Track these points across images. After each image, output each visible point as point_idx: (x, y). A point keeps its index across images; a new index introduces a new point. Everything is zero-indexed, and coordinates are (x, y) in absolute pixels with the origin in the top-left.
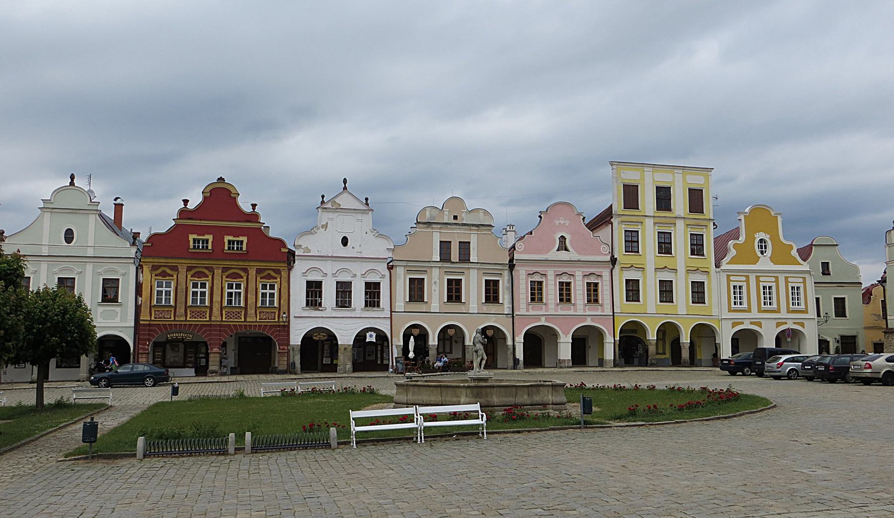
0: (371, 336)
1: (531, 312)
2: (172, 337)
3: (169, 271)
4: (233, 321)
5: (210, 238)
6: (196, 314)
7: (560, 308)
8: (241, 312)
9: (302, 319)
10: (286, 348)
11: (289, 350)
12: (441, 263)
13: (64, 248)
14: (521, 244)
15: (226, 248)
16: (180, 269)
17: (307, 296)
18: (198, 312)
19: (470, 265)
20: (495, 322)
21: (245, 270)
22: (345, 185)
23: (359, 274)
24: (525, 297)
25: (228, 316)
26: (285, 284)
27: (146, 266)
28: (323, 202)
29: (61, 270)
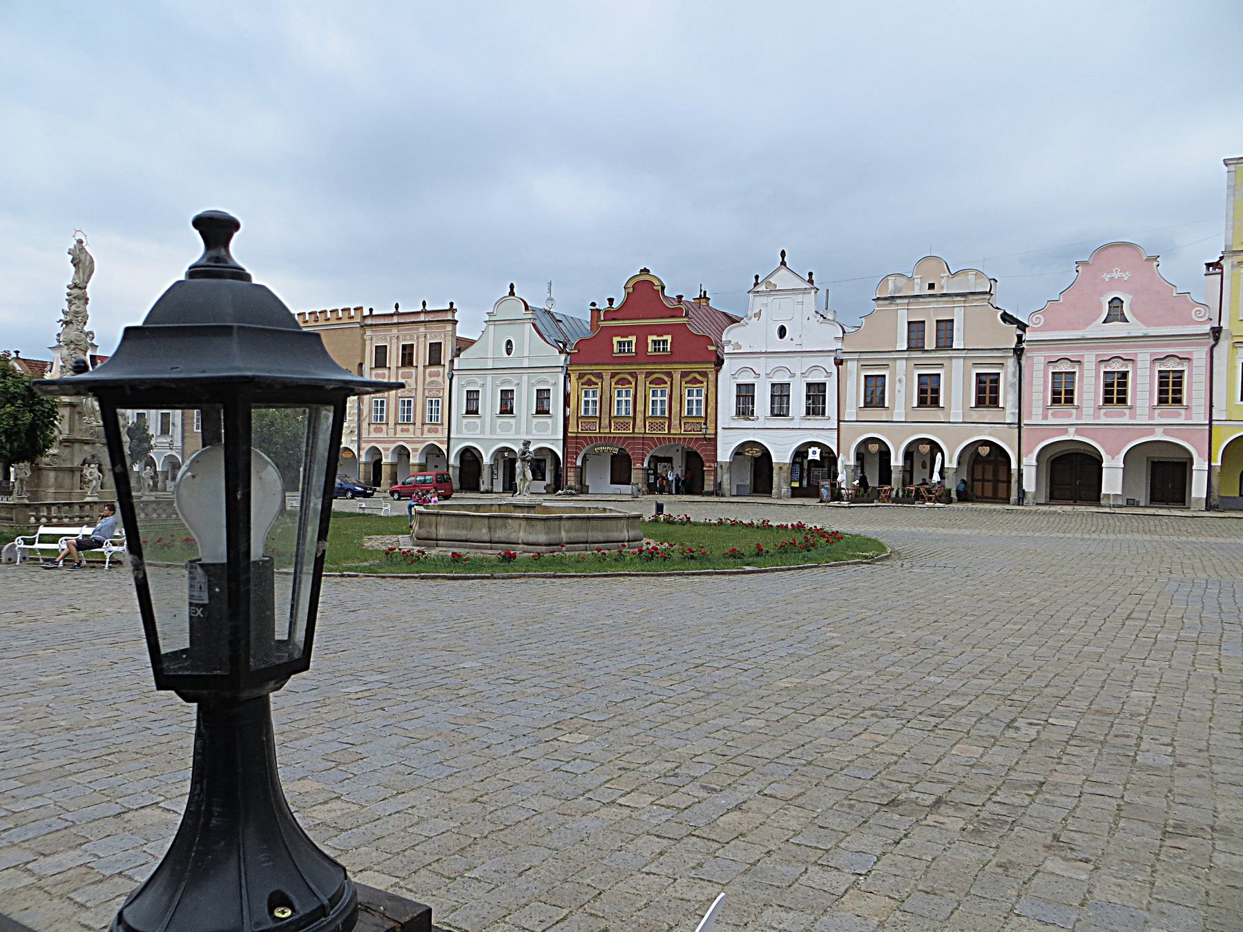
0: (814, 453)
1: (1051, 420)
7: (1053, 414)
10: (712, 465)
11: (716, 468)
12: (908, 353)
14: (1038, 316)
17: (738, 403)
19: (951, 353)
20: (990, 434)
21: (670, 375)
22: (783, 258)
23: (798, 374)
24: (1041, 398)
26: (712, 389)
28: (756, 284)
29: (503, 383)
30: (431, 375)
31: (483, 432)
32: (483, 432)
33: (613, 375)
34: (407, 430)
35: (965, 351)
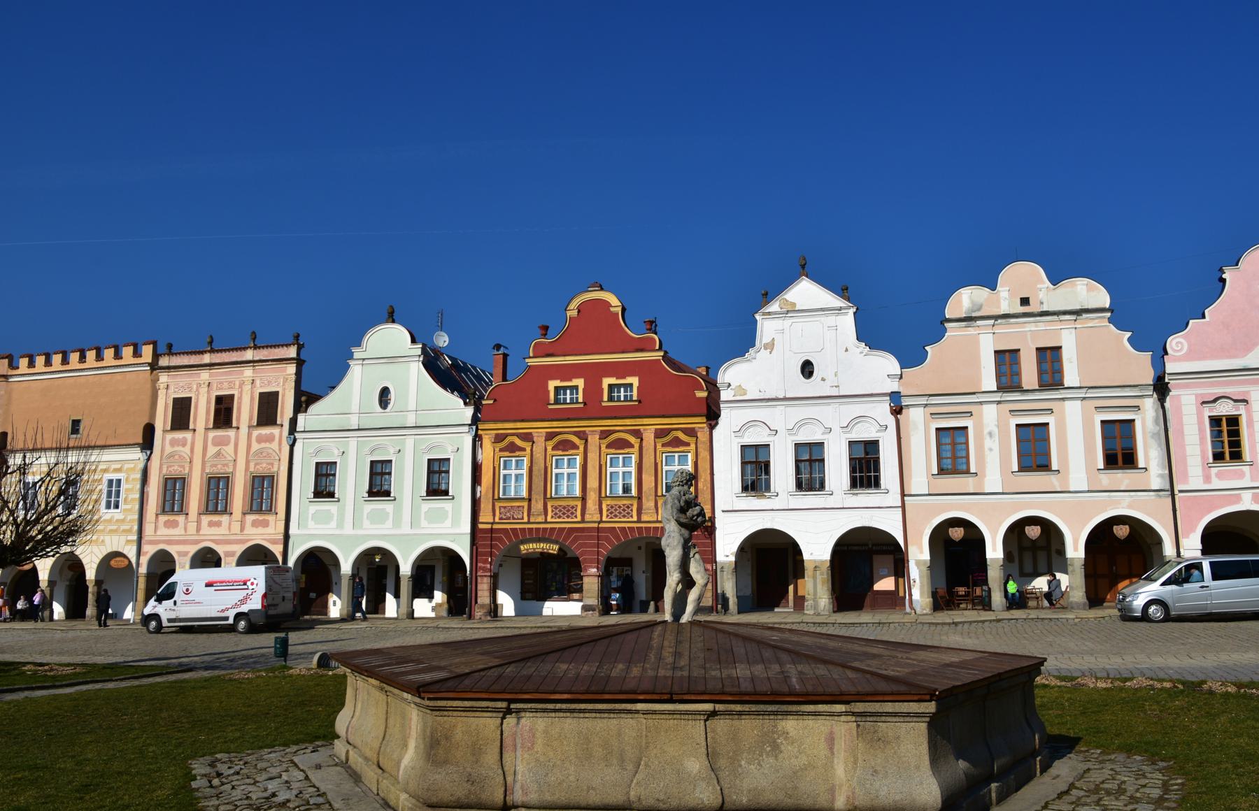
1: (1217, 483)
2: (527, 550)
3: (519, 442)
4: (620, 523)
5: (580, 382)
6: (560, 511)
8: (632, 505)
9: (737, 514)
12: (1000, 394)
13: (380, 417)
15: (605, 398)
16: (535, 439)
18: (564, 508)
20: (1130, 507)
21: (638, 434)
23: (836, 429)
25: (611, 513)
26: (704, 454)
27: (487, 436)
30: (260, 440)
31: (340, 525)
32: (340, 525)
33: (550, 437)
34: (218, 524)
35: (1085, 390)
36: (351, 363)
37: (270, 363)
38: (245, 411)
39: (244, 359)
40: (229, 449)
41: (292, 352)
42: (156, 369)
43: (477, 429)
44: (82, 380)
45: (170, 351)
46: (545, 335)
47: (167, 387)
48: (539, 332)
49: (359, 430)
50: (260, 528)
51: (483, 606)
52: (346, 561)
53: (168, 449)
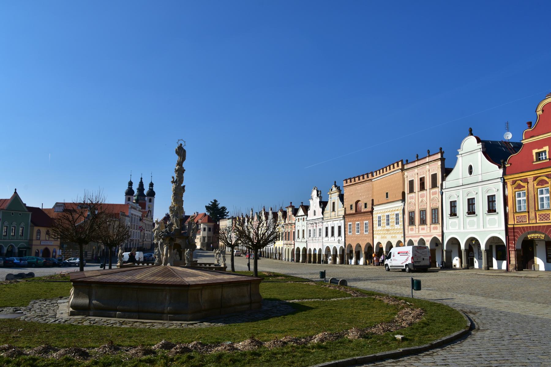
2: (531, 237)
3: (522, 184)
6: (542, 217)
18: (544, 215)
27: (509, 182)
31: (459, 228)
32: (459, 228)
33: (535, 178)
36: (458, 156)
37: (433, 162)
38: (428, 183)
39: (426, 162)
40: (425, 199)
41: (439, 156)
42: (403, 171)
43: (504, 180)
44: (387, 178)
45: (407, 163)
46: (530, 127)
47: (407, 177)
48: (527, 126)
49: (463, 185)
50: (435, 230)
51: (512, 265)
52: (462, 244)
53: (409, 201)
